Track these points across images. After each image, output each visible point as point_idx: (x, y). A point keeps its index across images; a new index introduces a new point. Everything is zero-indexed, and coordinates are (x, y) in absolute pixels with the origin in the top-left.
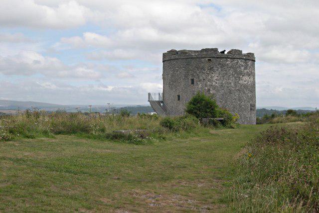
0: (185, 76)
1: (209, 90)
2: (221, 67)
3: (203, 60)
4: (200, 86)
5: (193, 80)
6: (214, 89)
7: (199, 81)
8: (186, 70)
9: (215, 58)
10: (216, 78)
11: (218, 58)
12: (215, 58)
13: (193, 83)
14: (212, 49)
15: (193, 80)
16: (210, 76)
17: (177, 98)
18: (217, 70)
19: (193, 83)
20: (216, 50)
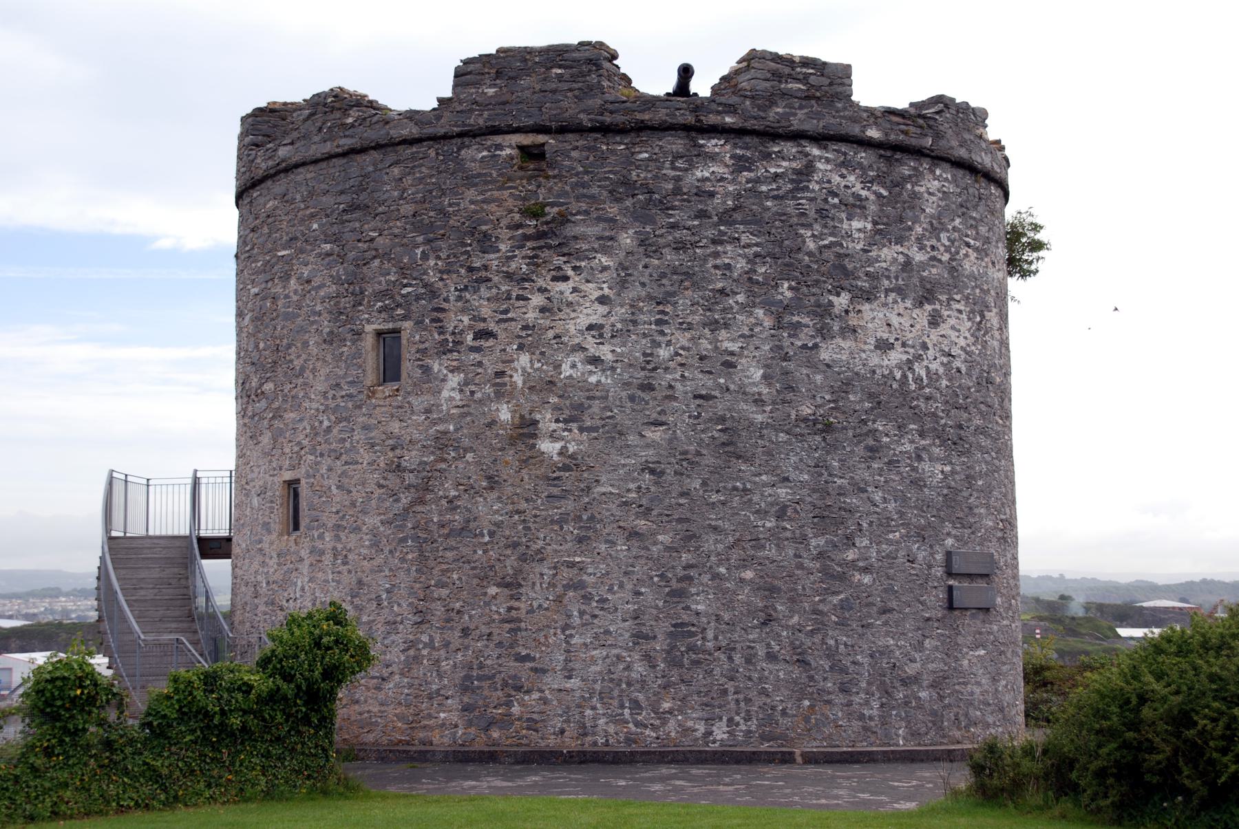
0: (337, 314)
1: (526, 429)
2: (641, 216)
3: (474, 154)
4: (451, 390)
5: (388, 339)
6: (573, 416)
7: (443, 350)
8: (342, 258)
9: (580, 130)
10: (591, 314)
11: (605, 130)
12: (580, 130)
13: (390, 371)
14: (556, 55)
15: (388, 339)
16: (537, 300)
17: (278, 516)
18: (606, 243)
19: (390, 371)
20: (592, 62)
